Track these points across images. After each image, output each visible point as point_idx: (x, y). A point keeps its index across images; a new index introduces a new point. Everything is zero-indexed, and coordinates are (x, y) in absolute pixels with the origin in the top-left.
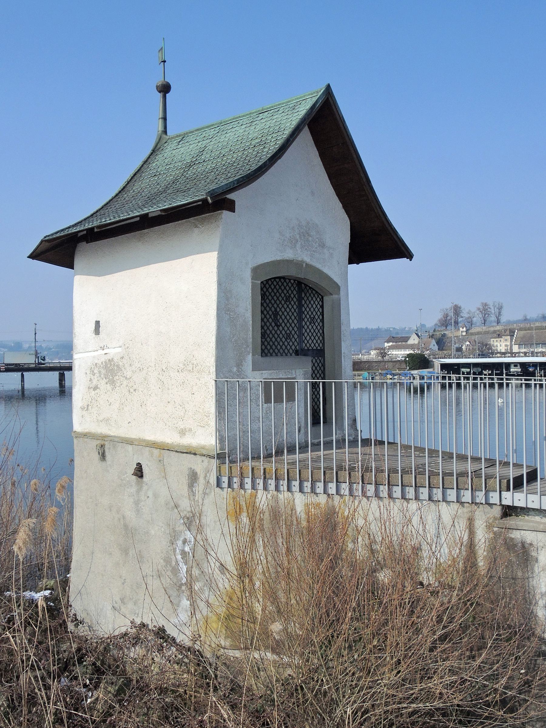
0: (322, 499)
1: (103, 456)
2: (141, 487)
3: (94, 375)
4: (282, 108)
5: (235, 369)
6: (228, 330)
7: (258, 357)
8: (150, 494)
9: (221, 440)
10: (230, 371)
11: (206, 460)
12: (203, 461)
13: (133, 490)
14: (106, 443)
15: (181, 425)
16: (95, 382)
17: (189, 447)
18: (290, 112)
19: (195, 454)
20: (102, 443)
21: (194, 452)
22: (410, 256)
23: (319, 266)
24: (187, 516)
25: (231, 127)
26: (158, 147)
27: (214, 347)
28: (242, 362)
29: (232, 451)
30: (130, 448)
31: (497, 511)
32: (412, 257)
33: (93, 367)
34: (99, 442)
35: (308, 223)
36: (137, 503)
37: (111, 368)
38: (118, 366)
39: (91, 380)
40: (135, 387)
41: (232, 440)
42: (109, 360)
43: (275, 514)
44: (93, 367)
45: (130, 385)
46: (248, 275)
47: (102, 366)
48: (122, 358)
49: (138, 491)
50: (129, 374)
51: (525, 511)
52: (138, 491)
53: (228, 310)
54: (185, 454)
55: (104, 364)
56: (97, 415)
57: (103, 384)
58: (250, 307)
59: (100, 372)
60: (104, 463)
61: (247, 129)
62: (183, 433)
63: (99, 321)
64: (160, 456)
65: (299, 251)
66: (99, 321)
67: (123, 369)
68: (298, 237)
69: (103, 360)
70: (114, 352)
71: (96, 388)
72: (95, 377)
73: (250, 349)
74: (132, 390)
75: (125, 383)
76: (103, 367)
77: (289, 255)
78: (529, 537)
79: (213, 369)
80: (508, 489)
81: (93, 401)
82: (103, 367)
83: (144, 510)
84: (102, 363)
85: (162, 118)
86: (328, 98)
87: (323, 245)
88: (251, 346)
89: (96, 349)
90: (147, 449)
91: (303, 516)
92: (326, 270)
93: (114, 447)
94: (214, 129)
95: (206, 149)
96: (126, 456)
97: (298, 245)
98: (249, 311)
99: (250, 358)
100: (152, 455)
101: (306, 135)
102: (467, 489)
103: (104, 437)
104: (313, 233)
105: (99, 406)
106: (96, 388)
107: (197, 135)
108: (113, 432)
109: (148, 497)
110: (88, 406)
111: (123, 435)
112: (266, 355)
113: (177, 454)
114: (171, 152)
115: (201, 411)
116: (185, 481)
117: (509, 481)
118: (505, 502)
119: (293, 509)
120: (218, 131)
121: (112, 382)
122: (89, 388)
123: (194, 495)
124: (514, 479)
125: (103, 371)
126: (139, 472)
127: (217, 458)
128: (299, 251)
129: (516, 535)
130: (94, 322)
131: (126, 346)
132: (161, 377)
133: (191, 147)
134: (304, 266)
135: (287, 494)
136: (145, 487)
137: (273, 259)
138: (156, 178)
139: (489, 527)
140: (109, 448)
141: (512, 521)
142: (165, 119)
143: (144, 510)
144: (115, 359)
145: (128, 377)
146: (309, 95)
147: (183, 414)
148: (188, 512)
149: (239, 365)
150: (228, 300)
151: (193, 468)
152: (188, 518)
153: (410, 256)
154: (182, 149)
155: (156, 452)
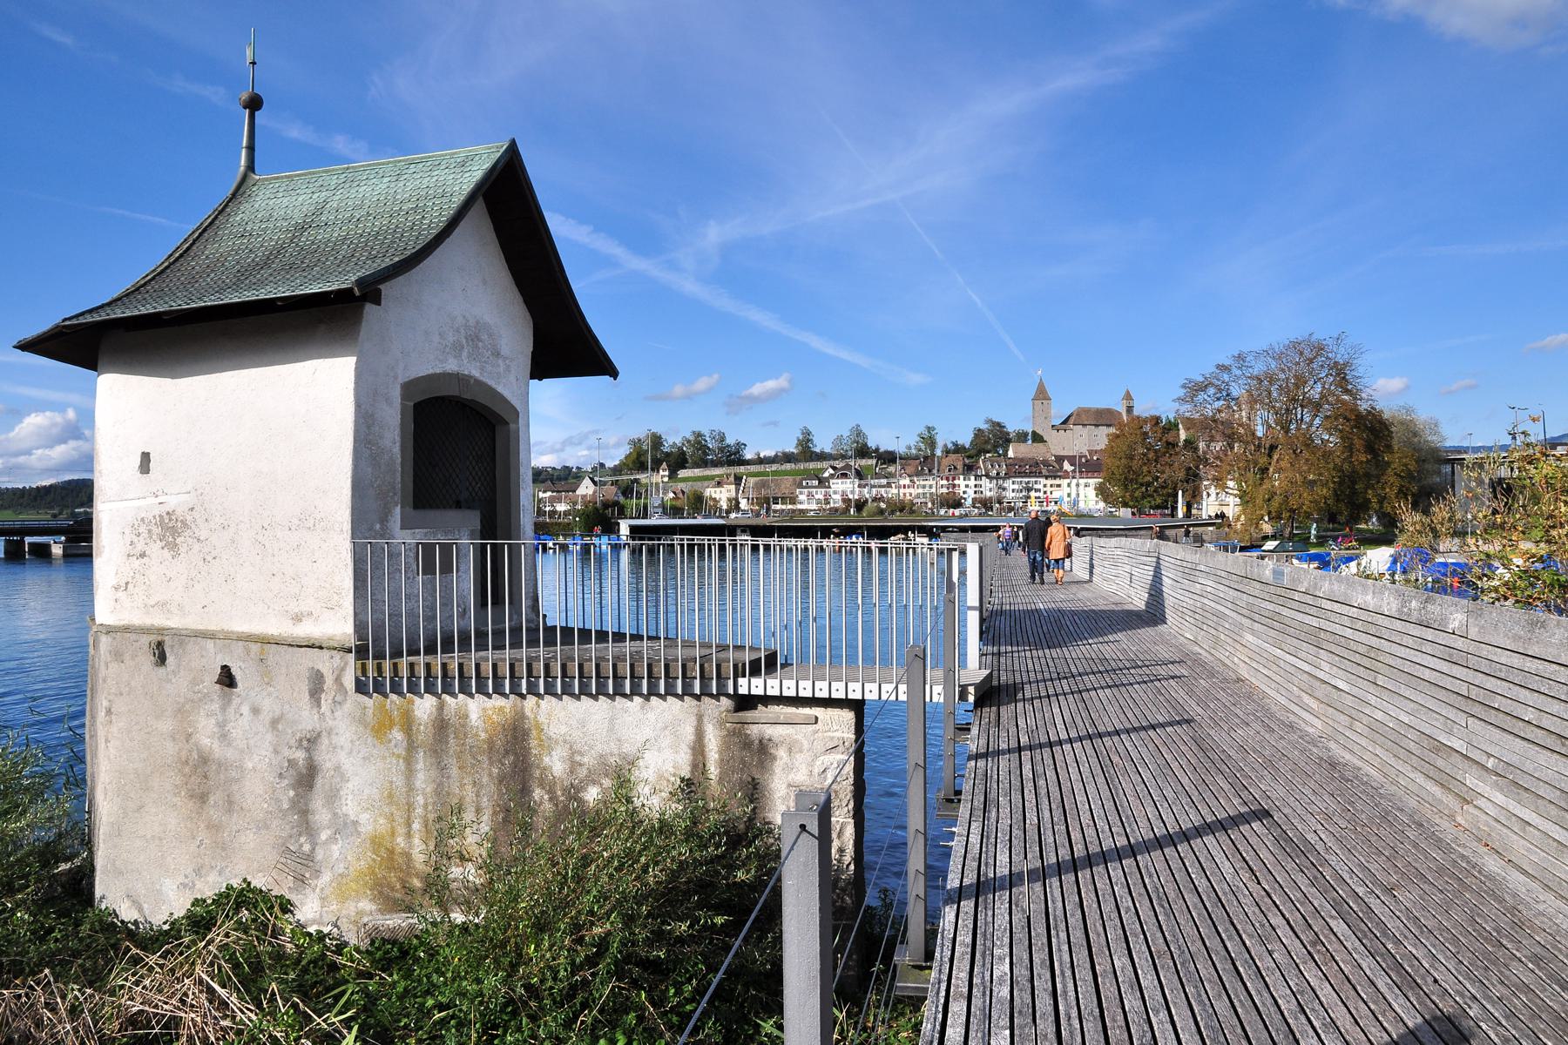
1: (162, 659)
2: (230, 701)
3: (139, 535)
4: (445, 162)
5: (378, 526)
6: (370, 469)
7: (409, 510)
8: (245, 709)
9: (360, 627)
10: (370, 529)
11: (337, 655)
12: (332, 657)
13: (215, 706)
14: (166, 638)
15: (294, 608)
16: (140, 547)
17: (309, 639)
18: (457, 170)
19: (321, 648)
20: (160, 638)
21: (318, 645)
22: (613, 373)
24: (308, 736)
27: (350, 494)
28: (387, 516)
29: (378, 639)
30: (210, 644)
33: (136, 523)
34: (154, 638)
35: (477, 323)
36: (221, 725)
37: (170, 525)
38: (184, 523)
39: (132, 543)
40: (214, 553)
41: (379, 627)
42: (168, 513)
43: (441, 725)
44: (136, 523)
45: (206, 550)
46: (396, 393)
47: (154, 522)
48: (192, 509)
49: (224, 709)
50: (203, 535)
51: (766, 700)
52: (224, 709)
53: (369, 443)
55: (158, 519)
56: (144, 597)
57: (155, 549)
59: (150, 531)
60: (162, 670)
61: (393, 185)
62: (298, 618)
63: (148, 454)
64: (261, 653)
65: (465, 362)
66: (148, 454)
67: (193, 526)
68: (464, 341)
69: (157, 513)
70: (174, 502)
71: (143, 555)
72: (141, 538)
73: (398, 498)
74: (209, 558)
75: (197, 547)
76: (156, 524)
77: (451, 366)
79: (347, 527)
80: (744, 676)
81: (137, 576)
82: (156, 524)
83: (234, 734)
84: (154, 517)
86: (512, 158)
87: (497, 354)
88: (399, 494)
89: (142, 496)
90: (240, 643)
91: (479, 723)
92: (500, 389)
93: (181, 643)
95: (328, 206)
96: (202, 656)
97: (465, 354)
98: (398, 444)
99: (398, 510)
100: (248, 652)
101: (480, 207)
103: (161, 631)
104: (485, 337)
105: (148, 583)
106: (143, 555)
108: (174, 622)
109: (241, 715)
110: (127, 584)
111: (194, 626)
112: (424, 507)
113: (290, 649)
114: (266, 202)
115: (327, 585)
116: (304, 687)
117: (744, 665)
118: (743, 691)
119: (466, 716)
121: (173, 547)
122: (129, 555)
123: (319, 706)
124: (750, 662)
125: (157, 530)
126: (227, 679)
127: (357, 652)
128: (465, 362)
129: (754, 731)
130: (140, 454)
131: (199, 492)
132: (260, 538)
133: (300, 199)
134: (472, 381)
136: (236, 701)
137: (431, 371)
139: (721, 724)
140: (172, 646)
141: (749, 715)
143: (234, 734)
144: (179, 512)
145: (202, 538)
147: (298, 592)
149: (384, 519)
150: (369, 427)
151: (316, 667)
152: (309, 740)
153: (613, 373)
154: (285, 200)
155: (255, 648)
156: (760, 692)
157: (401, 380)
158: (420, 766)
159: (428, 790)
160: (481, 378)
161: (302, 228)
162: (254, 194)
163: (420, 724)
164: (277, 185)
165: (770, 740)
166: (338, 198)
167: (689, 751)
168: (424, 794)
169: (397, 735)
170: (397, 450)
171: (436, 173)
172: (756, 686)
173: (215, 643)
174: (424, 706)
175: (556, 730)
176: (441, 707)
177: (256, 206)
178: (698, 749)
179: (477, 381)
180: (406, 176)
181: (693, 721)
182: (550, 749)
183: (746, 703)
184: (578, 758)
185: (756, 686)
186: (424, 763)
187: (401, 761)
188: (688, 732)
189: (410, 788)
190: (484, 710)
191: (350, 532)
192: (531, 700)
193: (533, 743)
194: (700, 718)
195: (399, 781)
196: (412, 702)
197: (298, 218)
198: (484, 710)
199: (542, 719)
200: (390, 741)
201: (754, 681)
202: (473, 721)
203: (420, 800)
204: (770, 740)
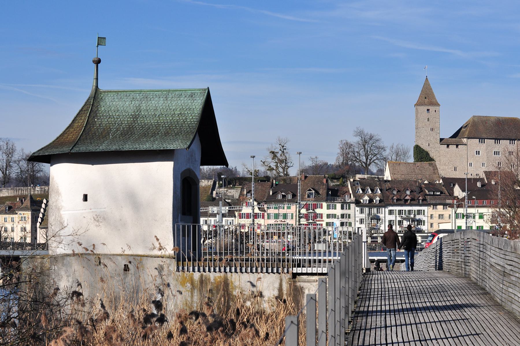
0: (222, 274)
11: (169, 260)
21: (162, 256)
23: (194, 171)
24: (158, 286)
25: (152, 97)
26: (96, 95)
31: (290, 276)
32: (228, 166)
52: (125, 278)
54: (156, 258)
58: (180, 192)
78: (302, 284)
85: (96, 79)
94: (138, 95)
102: (280, 267)
107: (125, 95)
113: (151, 258)
120: (142, 97)
129: (298, 284)
135: (207, 273)
138: (113, 120)
140: (104, 259)
142: (97, 79)
146: (198, 90)
148: (158, 284)
149: (178, 218)
156: (300, 272)
157: (180, 172)
158: (196, 294)
159: (198, 302)
160: (193, 170)
161: (135, 117)
162: (104, 98)
163: (195, 281)
164: (112, 95)
165: (303, 287)
166: (144, 105)
167: (278, 291)
168: (197, 303)
169: (189, 285)
170: (180, 195)
171: (182, 99)
172: (299, 270)
173: (121, 258)
174: (197, 276)
175: (237, 284)
176: (202, 275)
177: (108, 104)
178: (280, 290)
179: (193, 171)
180: (169, 99)
181: (279, 281)
182: (235, 289)
183: (295, 275)
184: (244, 292)
185: (299, 270)
186: (197, 293)
187: (190, 293)
188: (277, 285)
189: (192, 301)
190: (215, 277)
191: (172, 221)
192: (229, 274)
193: (230, 287)
194: (281, 280)
195: (189, 299)
196: (193, 274)
197: (131, 112)
198: (215, 277)
199: (233, 280)
200: (186, 286)
201: (298, 269)
202: (212, 281)
203: (195, 305)
204: (303, 287)
